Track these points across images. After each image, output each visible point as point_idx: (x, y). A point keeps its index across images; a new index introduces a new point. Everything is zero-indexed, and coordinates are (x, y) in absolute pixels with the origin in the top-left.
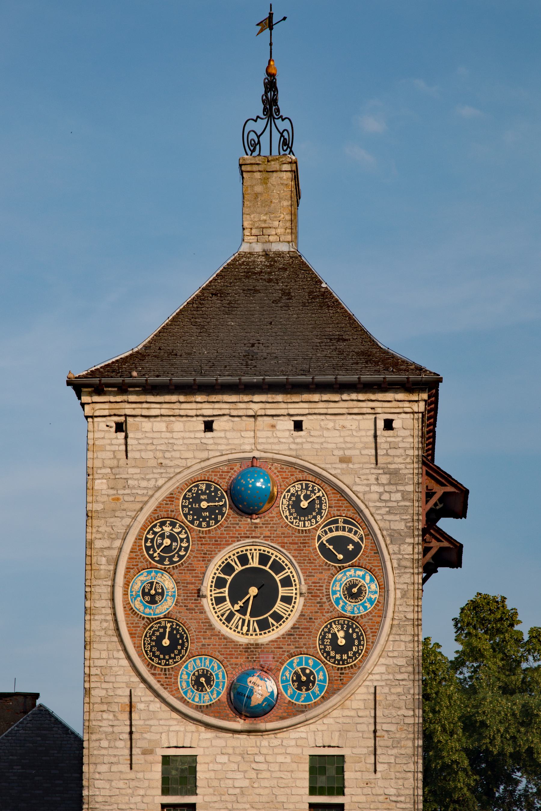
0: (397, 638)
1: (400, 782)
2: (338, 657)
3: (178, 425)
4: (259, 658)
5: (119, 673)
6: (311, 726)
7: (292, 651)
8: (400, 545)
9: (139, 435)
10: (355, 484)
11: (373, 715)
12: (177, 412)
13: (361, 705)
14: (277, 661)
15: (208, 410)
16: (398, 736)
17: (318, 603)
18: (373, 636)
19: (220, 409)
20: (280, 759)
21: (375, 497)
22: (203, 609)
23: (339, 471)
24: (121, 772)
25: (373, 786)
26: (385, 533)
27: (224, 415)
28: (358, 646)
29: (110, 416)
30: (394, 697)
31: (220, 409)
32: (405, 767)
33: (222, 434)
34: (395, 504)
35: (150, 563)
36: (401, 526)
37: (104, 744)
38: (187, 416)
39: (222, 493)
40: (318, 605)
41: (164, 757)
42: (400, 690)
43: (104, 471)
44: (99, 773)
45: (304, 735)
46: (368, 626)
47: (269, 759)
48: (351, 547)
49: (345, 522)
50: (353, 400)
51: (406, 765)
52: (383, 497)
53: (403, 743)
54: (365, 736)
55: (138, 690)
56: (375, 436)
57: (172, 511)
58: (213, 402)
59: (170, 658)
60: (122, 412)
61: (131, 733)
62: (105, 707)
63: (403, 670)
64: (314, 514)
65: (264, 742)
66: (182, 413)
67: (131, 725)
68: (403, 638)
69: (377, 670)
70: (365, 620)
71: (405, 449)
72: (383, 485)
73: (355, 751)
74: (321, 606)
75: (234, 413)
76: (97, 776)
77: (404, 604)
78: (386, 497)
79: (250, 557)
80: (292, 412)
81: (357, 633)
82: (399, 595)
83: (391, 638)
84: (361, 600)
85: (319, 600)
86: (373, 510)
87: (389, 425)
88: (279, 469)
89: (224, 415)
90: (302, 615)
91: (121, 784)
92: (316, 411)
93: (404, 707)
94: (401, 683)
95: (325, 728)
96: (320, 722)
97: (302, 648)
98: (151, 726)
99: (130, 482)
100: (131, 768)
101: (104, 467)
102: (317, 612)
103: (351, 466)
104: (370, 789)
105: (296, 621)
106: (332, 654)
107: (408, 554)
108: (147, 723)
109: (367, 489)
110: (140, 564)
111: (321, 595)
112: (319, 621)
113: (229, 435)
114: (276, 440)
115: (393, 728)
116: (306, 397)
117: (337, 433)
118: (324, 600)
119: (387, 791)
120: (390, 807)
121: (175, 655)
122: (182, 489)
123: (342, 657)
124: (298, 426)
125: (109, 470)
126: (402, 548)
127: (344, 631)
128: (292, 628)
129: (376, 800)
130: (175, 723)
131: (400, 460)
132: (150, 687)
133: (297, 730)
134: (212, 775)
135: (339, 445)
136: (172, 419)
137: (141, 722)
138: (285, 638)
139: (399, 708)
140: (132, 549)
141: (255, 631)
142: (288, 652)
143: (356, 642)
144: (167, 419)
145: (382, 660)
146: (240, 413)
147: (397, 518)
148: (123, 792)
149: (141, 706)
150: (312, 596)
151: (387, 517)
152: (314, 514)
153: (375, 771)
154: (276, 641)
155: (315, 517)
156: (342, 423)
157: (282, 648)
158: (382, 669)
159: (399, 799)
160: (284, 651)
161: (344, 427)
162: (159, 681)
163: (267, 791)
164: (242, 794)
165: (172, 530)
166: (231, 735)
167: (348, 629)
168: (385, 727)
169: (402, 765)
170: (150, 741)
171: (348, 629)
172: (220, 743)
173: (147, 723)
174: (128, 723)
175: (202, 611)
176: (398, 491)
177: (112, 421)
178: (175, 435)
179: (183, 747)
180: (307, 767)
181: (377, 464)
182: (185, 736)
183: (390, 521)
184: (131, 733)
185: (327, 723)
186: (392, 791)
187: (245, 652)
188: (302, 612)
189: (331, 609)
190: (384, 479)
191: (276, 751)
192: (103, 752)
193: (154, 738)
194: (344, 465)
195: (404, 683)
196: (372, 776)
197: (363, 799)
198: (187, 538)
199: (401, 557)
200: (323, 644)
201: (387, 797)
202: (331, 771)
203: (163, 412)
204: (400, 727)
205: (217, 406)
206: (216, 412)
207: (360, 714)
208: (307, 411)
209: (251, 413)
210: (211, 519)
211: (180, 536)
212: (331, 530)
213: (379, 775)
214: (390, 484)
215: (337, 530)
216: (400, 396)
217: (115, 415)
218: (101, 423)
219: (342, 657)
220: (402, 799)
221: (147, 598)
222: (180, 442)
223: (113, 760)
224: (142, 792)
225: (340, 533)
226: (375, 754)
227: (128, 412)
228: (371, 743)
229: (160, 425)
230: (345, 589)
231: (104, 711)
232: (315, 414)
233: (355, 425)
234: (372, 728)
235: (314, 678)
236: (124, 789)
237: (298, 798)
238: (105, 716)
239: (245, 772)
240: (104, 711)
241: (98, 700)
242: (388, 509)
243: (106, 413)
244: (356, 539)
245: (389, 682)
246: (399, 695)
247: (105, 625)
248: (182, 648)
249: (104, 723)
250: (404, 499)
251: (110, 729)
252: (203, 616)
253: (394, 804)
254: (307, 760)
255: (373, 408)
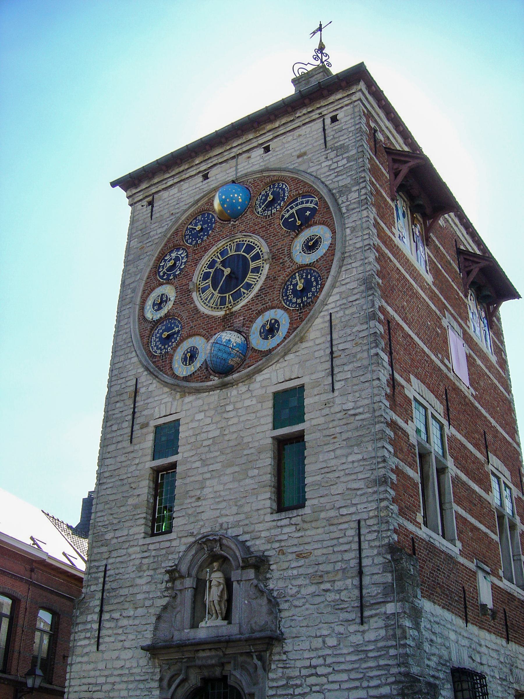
0: (349, 267)
1: (357, 395)
2: (299, 301)
3: (185, 185)
4: (233, 323)
5: (130, 369)
6: (274, 366)
7: (259, 308)
8: (347, 195)
9: (161, 202)
10: (310, 167)
11: (329, 339)
12: (184, 177)
13: (318, 334)
14: (247, 321)
15: (203, 167)
16: (353, 351)
17: (280, 264)
18: (327, 273)
19: (212, 162)
20: (247, 403)
21: (327, 169)
22: (193, 300)
23: (297, 165)
24: (124, 448)
25: (331, 404)
26: (334, 191)
27: (215, 165)
28: (316, 286)
29: (144, 198)
30: (347, 318)
31: (212, 162)
32: (362, 379)
33: (214, 178)
34: (342, 168)
35: (159, 281)
36: (348, 180)
37: (115, 428)
38: (191, 177)
39: (212, 215)
40: (281, 265)
41: (156, 427)
42: (354, 309)
43: (137, 234)
44: (109, 453)
45: (268, 376)
46: (323, 266)
47: (239, 405)
48: (308, 213)
49: (304, 197)
50: (304, 114)
51: (363, 376)
52: (332, 167)
53: (358, 356)
54: (322, 361)
55: (142, 377)
56: (324, 130)
57: (176, 241)
58: (206, 160)
59: (169, 346)
60: (151, 193)
61: (134, 413)
62: (117, 399)
63: (356, 291)
64: (279, 202)
65: (233, 392)
66: (187, 176)
67: (134, 408)
68: (354, 265)
69: (331, 299)
70: (320, 262)
71: (347, 129)
72: (332, 159)
73: (314, 377)
74: (284, 265)
75: (220, 161)
76: (109, 456)
77: (354, 238)
78: (335, 166)
79: (229, 251)
80: (261, 142)
81: (315, 276)
82: (348, 231)
83: (343, 269)
84: (317, 249)
85: (281, 261)
86: (323, 180)
87: (334, 119)
88: (252, 182)
89: (215, 165)
90: (268, 277)
91: (123, 458)
92: (278, 134)
93: (359, 324)
94: (354, 303)
95: (285, 364)
96: (281, 360)
97: (268, 303)
98: (148, 403)
99: (152, 233)
100: (131, 442)
101: (137, 231)
102: (280, 271)
103: (305, 157)
104: (328, 409)
105: (263, 284)
106: (294, 300)
107: (355, 199)
108: (146, 402)
109: (320, 167)
110: (153, 285)
111: (283, 257)
112: (281, 277)
113: (218, 176)
114: (251, 165)
115: (347, 345)
116: (269, 127)
117: (295, 141)
118: (286, 259)
119: (345, 407)
120: (349, 422)
121: (173, 343)
122: (184, 224)
123: (302, 300)
124: (267, 149)
125: (140, 232)
126: (349, 197)
127: (304, 278)
128: (259, 291)
129: (335, 419)
130: (166, 396)
131: (345, 137)
132: (151, 373)
133: (262, 373)
134: (191, 432)
135: (296, 149)
136: (182, 183)
137: (142, 403)
138: (253, 300)
139: (354, 326)
140: (148, 276)
141: (230, 303)
142: (256, 310)
143: (314, 284)
144: (178, 185)
145: (336, 290)
146: (225, 159)
147: (344, 176)
148: (124, 464)
149: (142, 390)
150: (276, 260)
151: (336, 179)
152: (279, 202)
153: (333, 390)
154: (247, 305)
155: (280, 204)
156: (298, 134)
157: (251, 309)
158: (337, 297)
159: (358, 411)
160: (254, 311)
161: (300, 135)
162: (157, 367)
163: (235, 435)
164: (214, 443)
165: (177, 254)
166: (207, 393)
167: (307, 276)
168: (341, 347)
169: (358, 377)
170: (146, 416)
171: (307, 276)
172: (200, 402)
173: (146, 402)
174: (132, 406)
175: (192, 302)
176: (343, 159)
177: (145, 203)
178: (183, 192)
179: (171, 414)
180: (270, 404)
181: (326, 147)
182: (172, 405)
183: (338, 181)
184: (134, 413)
185: (288, 359)
186: (350, 405)
187: (222, 322)
188: (267, 275)
189: (292, 265)
190: (332, 155)
191: (244, 397)
192: (114, 434)
193: (150, 413)
194: (300, 159)
195: (357, 302)
196: (331, 395)
197: (321, 420)
198: (187, 256)
199: (349, 203)
200: (286, 295)
201: (346, 412)
202: (294, 402)
203: (176, 180)
204: (356, 342)
205: (209, 161)
206: (209, 165)
207: (318, 342)
208: (271, 137)
209: (232, 155)
210: (204, 235)
211: (182, 256)
212: (292, 208)
213: (336, 393)
214: (337, 156)
215: (297, 205)
216: (339, 96)
217: (147, 197)
218: (139, 206)
219: (302, 300)
220: (361, 410)
221: (156, 308)
222: (186, 195)
223: (120, 439)
224: (137, 461)
225: (300, 207)
226: (332, 375)
227: (154, 191)
228: (328, 365)
229: (174, 191)
230: (304, 246)
231: (117, 402)
232: (278, 136)
233: (309, 129)
234: (328, 351)
235: (279, 325)
236: (125, 461)
237: (261, 435)
238: (118, 405)
239: (217, 423)
240: (117, 402)
241: (115, 394)
242: (336, 174)
243: (141, 197)
244: (312, 206)
245: (342, 307)
246: (353, 314)
247: (125, 336)
248: (178, 336)
249: (116, 411)
250: (348, 162)
251: (120, 415)
252: (192, 305)
253: (353, 418)
254: (271, 397)
255: (320, 113)
